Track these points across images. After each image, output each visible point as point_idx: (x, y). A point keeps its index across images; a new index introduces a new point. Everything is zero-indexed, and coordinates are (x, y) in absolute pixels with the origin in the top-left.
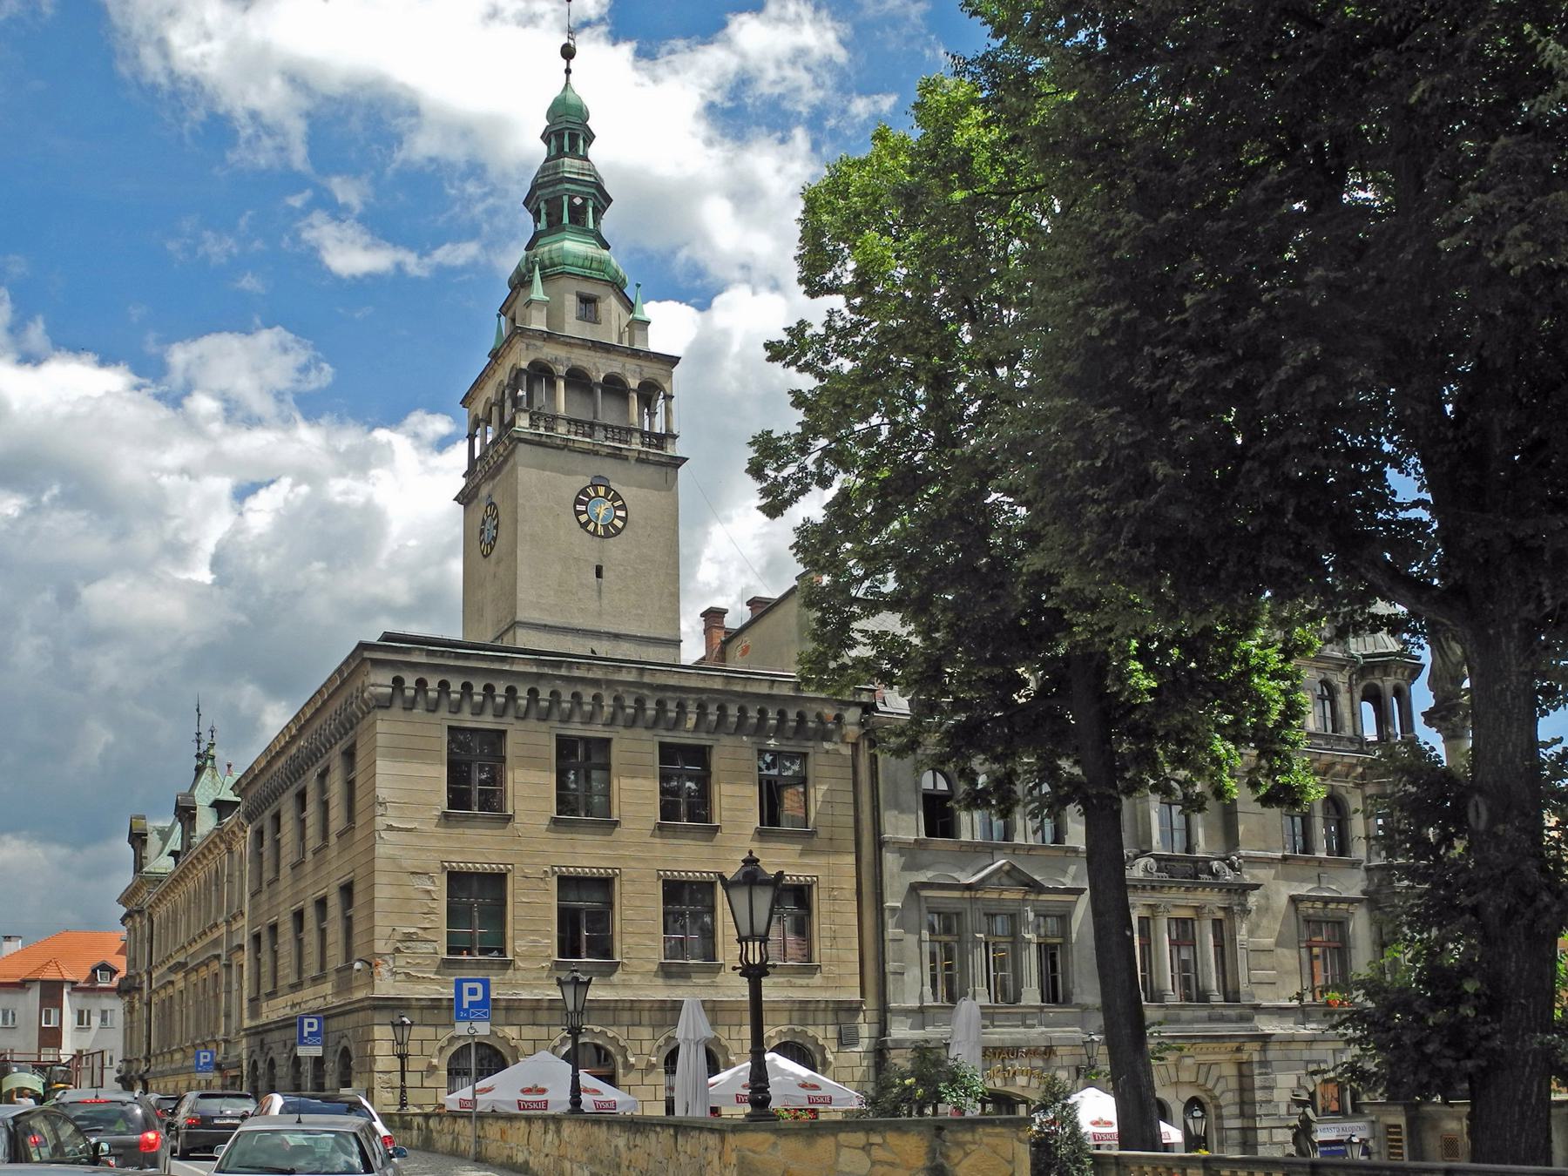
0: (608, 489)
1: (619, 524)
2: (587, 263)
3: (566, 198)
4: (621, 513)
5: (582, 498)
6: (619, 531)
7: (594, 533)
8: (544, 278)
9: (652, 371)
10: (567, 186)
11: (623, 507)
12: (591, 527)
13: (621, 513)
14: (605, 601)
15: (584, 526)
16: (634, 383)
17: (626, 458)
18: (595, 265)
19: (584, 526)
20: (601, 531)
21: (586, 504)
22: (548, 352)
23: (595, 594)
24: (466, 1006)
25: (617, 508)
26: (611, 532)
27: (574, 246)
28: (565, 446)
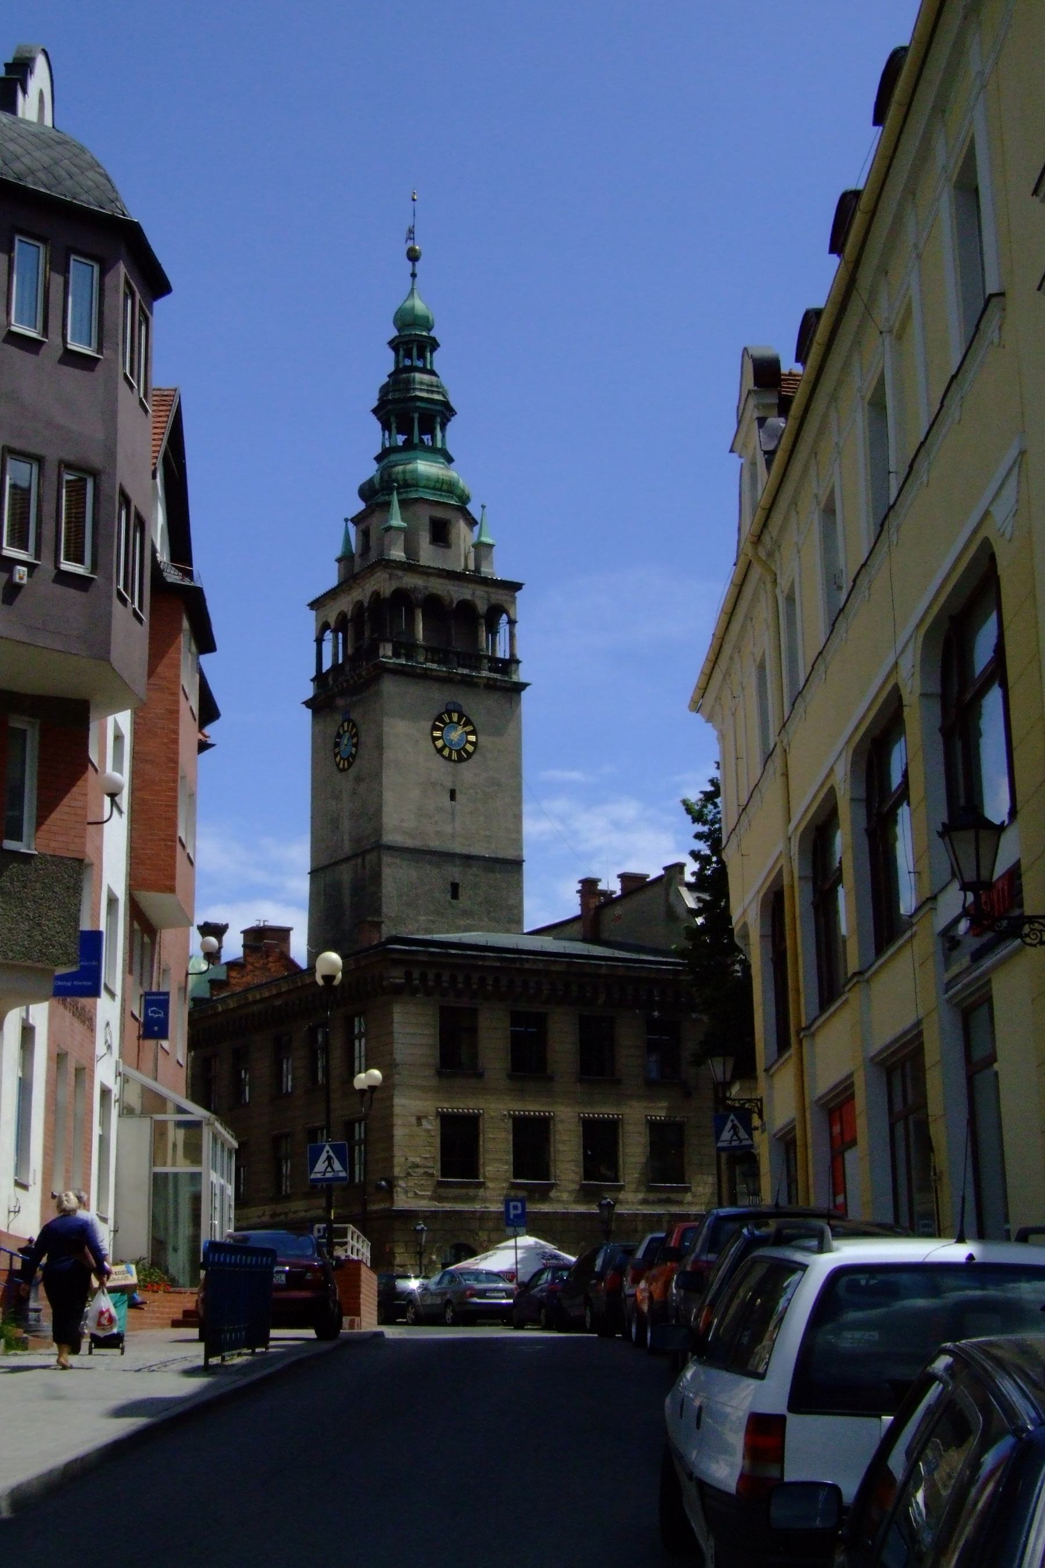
2: (438, 485)
6: (470, 755)
7: (449, 759)
8: (403, 504)
9: (499, 596)
10: (419, 404)
12: (446, 752)
15: (440, 751)
16: (482, 607)
18: (445, 487)
19: (440, 751)
20: (454, 756)
22: (411, 581)
24: (512, 1217)
26: (463, 756)
27: (425, 467)
28: (425, 676)
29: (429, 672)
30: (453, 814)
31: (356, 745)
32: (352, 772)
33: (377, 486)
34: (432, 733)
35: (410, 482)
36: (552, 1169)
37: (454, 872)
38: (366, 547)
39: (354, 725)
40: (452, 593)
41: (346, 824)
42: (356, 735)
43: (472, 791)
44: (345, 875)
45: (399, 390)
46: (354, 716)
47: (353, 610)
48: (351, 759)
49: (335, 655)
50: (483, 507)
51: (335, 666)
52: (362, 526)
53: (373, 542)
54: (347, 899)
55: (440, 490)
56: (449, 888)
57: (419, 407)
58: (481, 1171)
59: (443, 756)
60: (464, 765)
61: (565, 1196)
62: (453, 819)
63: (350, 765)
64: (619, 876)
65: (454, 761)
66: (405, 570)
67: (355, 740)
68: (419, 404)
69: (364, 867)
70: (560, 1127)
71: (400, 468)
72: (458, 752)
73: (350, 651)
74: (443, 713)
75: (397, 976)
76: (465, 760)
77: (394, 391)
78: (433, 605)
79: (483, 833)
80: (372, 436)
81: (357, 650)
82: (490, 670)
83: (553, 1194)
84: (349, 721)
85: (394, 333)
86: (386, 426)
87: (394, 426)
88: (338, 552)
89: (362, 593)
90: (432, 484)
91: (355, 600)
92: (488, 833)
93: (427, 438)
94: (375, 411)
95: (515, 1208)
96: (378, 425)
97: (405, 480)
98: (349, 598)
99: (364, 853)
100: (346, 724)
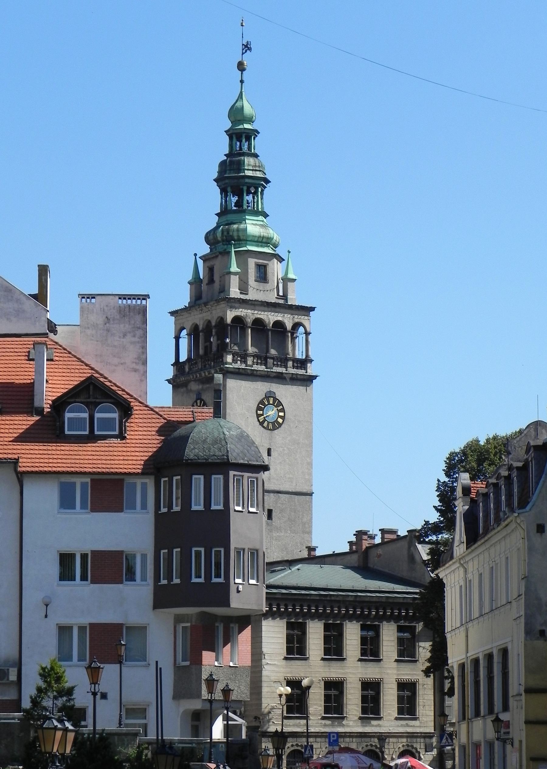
0: (275, 399)
1: (280, 420)
2: (260, 240)
3: (245, 188)
4: (281, 414)
5: (261, 406)
6: (280, 425)
7: (267, 428)
10: (247, 180)
11: (283, 410)
12: (265, 424)
13: (281, 414)
16: (289, 326)
17: (285, 378)
19: (261, 424)
20: (271, 426)
21: (262, 409)
25: (279, 411)
26: (276, 426)
29: (255, 372)
33: (219, 239)
34: (257, 412)
35: (242, 238)
38: (211, 281)
43: (281, 449)
45: (233, 170)
49: (189, 351)
51: (189, 359)
52: (209, 264)
53: (216, 278)
55: (261, 242)
57: (247, 183)
59: (264, 427)
65: (270, 430)
68: (247, 180)
71: (235, 226)
73: (201, 352)
74: (264, 399)
76: (278, 428)
77: (230, 170)
79: (288, 476)
82: (294, 367)
84: (201, 400)
86: (224, 191)
88: (190, 276)
90: (256, 239)
92: (291, 476)
97: (238, 236)
100: (199, 401)
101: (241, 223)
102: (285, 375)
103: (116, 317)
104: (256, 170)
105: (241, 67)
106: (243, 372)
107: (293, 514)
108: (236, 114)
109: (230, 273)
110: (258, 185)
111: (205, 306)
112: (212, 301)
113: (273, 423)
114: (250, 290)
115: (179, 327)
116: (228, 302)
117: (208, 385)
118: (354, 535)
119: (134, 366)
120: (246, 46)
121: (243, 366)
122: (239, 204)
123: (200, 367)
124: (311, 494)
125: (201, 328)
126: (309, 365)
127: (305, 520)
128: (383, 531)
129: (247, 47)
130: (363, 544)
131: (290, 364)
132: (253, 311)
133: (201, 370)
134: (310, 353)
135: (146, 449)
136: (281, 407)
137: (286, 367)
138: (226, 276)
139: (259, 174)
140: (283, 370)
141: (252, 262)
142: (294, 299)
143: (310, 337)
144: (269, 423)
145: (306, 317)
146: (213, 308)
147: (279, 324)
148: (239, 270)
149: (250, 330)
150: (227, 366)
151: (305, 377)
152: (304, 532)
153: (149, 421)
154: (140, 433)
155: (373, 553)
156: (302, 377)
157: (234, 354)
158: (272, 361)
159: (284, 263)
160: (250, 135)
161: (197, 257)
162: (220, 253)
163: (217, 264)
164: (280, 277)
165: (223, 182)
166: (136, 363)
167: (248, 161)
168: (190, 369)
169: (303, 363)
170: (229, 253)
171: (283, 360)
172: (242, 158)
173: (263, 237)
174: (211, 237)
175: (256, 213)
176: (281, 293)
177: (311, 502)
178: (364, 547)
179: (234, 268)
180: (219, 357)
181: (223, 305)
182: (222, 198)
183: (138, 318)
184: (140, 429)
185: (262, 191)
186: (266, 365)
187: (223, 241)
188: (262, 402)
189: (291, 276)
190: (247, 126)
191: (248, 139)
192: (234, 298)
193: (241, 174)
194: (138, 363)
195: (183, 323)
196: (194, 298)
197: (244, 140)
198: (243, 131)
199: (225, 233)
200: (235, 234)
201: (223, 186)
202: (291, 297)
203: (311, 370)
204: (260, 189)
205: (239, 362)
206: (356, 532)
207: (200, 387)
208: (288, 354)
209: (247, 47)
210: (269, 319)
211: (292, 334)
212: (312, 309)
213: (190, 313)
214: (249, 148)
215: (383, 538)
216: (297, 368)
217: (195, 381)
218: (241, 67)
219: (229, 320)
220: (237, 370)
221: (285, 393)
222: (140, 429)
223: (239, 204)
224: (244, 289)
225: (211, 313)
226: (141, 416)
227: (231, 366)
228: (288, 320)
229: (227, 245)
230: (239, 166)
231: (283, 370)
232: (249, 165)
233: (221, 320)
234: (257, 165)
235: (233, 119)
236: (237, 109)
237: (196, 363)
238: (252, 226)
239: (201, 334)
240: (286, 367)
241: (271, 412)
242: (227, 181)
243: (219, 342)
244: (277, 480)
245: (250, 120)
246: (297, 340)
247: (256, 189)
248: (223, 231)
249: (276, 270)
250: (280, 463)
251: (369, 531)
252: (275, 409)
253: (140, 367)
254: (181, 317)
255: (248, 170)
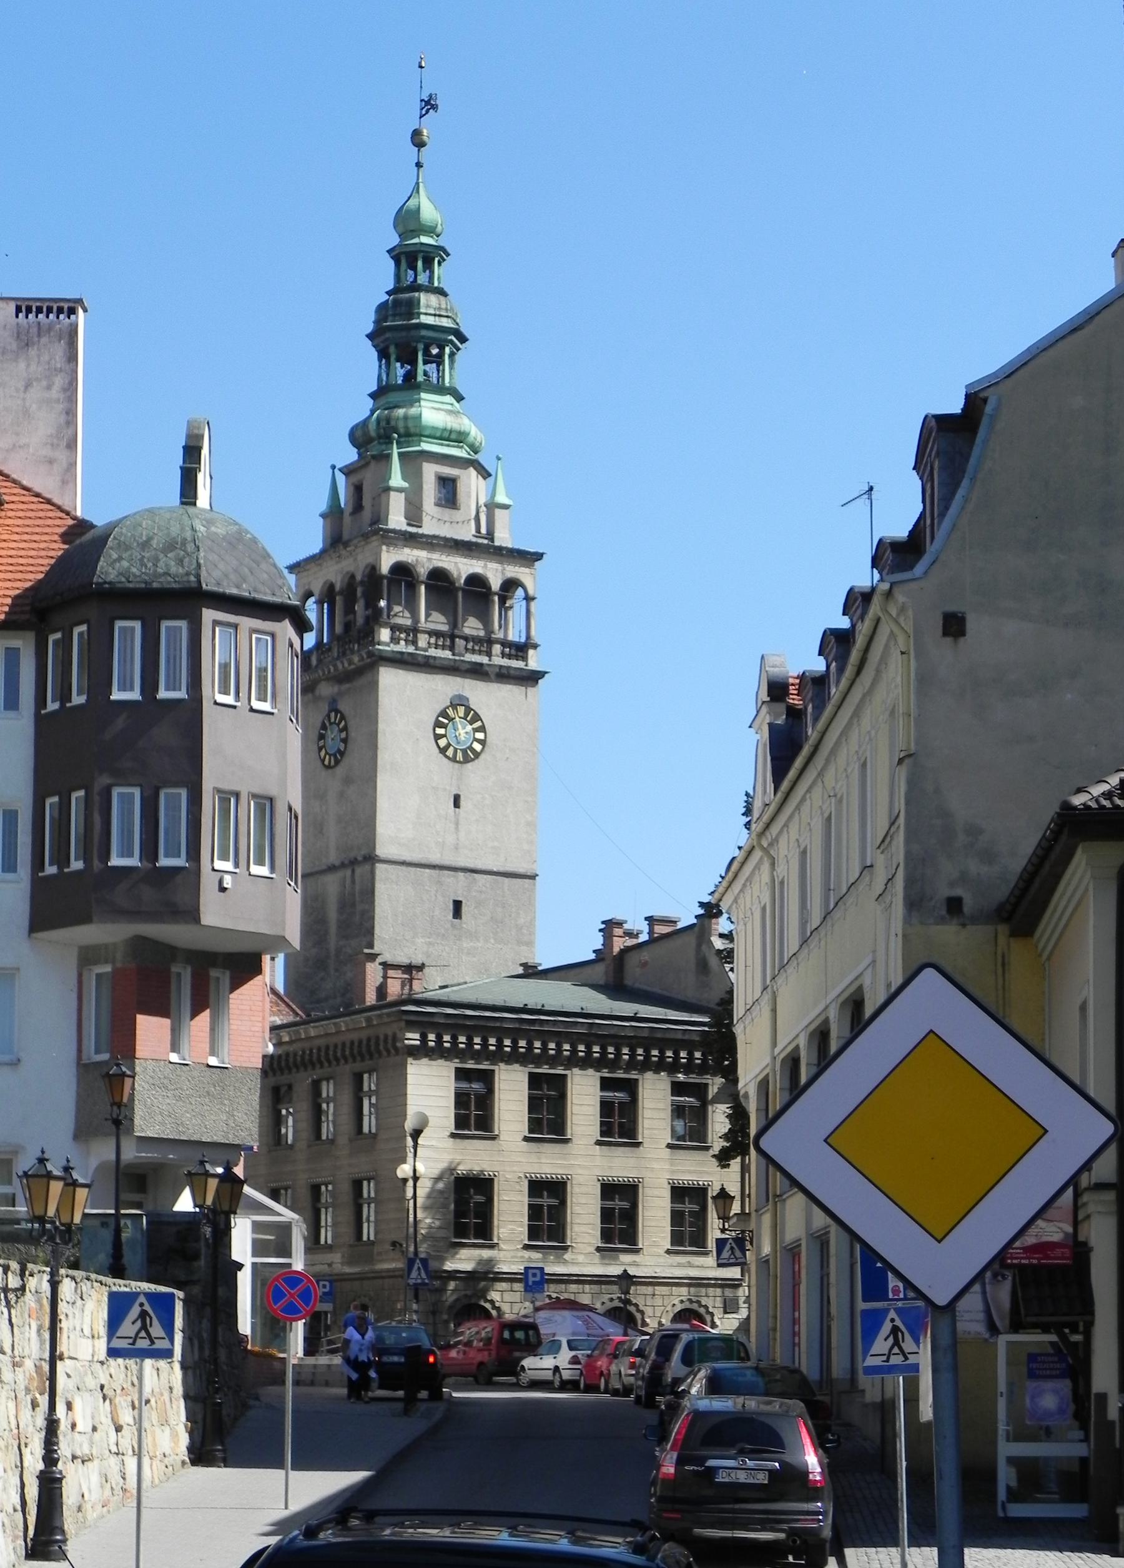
0: (468, 709)
1: (477, 747)
2: (446, 435)
3: (421, 346)
6: (477, 755)
7: (454, 759)
10: (424, 333)
11: (482, 729)
12: (450, 752)
14: (462, 834)
16: (495, 584)
23: (453, 826)
25: (476, 730)
26: (469, 756)
30: (457, 824)
31: (345, 741)
32: (340, 770)
33: (373, 434)
35: (412, 430)
36: (569, 1232)
37: (457, 886)
38: (358, 507)
39: (343, 718)
40: (460, 565)
41: (332, 831)
42: (345, 729)
44: (332, 885)
45: (400, 315)
46: (343, 706)
47: (342, 581)
48: (339, 756)
50: (499, 459)
53: (367, 502)
54: (333, 915)
56: (451, 907)
57: (423, 337)
58: (495, 1233)
60: (469, 765)
61: (581, 1258)
62: (457, 828)
63: (337, 762)
64: (646, 919)
65: (459, 762)
66: (406, 539)
67: (343, 735)
68: (424, 333)
69: (353, 882)
70: (576, 1189)
71: (401, 412)
72: (464, 751)
73: (339, 629)
75: (413, 1038)
76: (473, 760)
77: (394, 315)
78: (439, 579)
80: (365, 368)
81: (347, 626)
82: (503, 655)
83: (568, 1256)
84: (337, 711)
85: (394, 240)
87: (393, 358)
89: (354, 563)
90: (438, 434)
91: (347, 569)
92: (496, 844)
93: (432, 368)
94: (370, 336)
95: (534, 1275)
96: (374, 354)
98: (336, 567)
99: (353, 863)
100: (333, 715)
101: (412, 406)
102: (487, 668)
103: (9, 348)
104: (440, 316)
105: (417, 140)
106: (410, 659)
107: (499, 910)
108: (407, 221)
109: (388, 489)
110: (446, 340)
111: (345, 548)
112: (356, 537)
113: (464, 751)
114: (426, 519)
115: (302, 592)
116: (382, 536)
117: (347, 686)
118: (600, 930)
119: (46, 452)
120: (427, 103)
121: (411, 649)
122: (410, 377)
123: (336, 655)
124: (533, 877)
125: (338, 588)
126: (531, 652)
127: (521, 921)
128: (651, 920)
129: (429, 105)
130: (615, 944)
131: (497, 648)
132: (430, 555)
133: (338, 658)
134: (533, 633)
135: (19, 576)
136: (479, 724)
137: (489, 654)
138: (383, 495)
139: (445, 323)
140: (484, 660)
141: (430, 471)
142: (503, 538)
143: (533, 605)
144: (456, 750)
145: (527, 570)
146: (359, 550)
147: (476, 581)
148: (406, 485)
149: (423, 588)
150: (380, 647)
151: (524, 674)
152: (519, 942)
153: (40, 522)
154: (14, 545)
155: (632, 960)
156: (517, 673)
157: (394, 628)
158: (463, 642)
159: (491, 480)
160: (430, 256)
161: (336, 471)
162: (373, 457)
163: (368, 477)
164: (482, 501)
165: (382, 338)
166: (52, 445)
167: (427, 302)
168: (320, 661)
169: (520, 650)
170: (388, 457)
171: (485, 643)
172: (416, 294)
173: (451, 432)
174: (359, 433)
175: (440, 389)
176: (484, 531)
177: (533, 890)
178: (616, 950)
179: (396, 479)
180: (368, 634)
181: (374, 541)
182: (380, 366)
183: (59, 350)
184: (16, 537)
185: (452, 355)
186: (452, 648)
187: (379, 439)
188: (444, 714)
189: (501, 498)
190: (424, 239)
191: (428, 264)
192: (394, 531)
193: (414, 321)
194: (58, 445)
195: (309, 583)
196: (329, 541)
197: (420, 264)
198: (418, 248)
199: (383, 424)
200: (401, 424)
201: (382, 345)
202: (502, 535)
203: (534, 661)
204: (447, 350)
205: (402, 643)
206: (603, 922)
207: (336, 689)
208: (493, 632)
209: (429, 105)
210: (458, 570)
211: (503, 600)
212: (538, 556)
213: (320, 565)
214: (431, 278)
215: (651, 932)
216: (510, 657)
217: (328, 679)
218: (417, 140)
219: (385, 568)
220: (399, 656)
221: (484, 696)
222: (16, 537)
223: (410, 377)
224: (414, 514)
225: (355, 560)
226: (21, 514)
227: (387, 648)
228: (494, 573)
229: (386, 443)
230: (410, 308)
231: (484, 660)
232: (428, 306)
233: (373, 569)
234: (443, 306)
235: (401, 230)
236: (408, 211)
237: (329, 650)
238: (432, 411)
239: (337, 598)
240: (489, 654)
241: (464, 731)
242: (388, 335)
243: (369, 612)
244: (471, 850)
245: (431, 231)
246: (510, 613)
247: (442, 348)
248: (378, 420)
249: (472, 487)
250: (477, 820)
251: (626, 922)
252: (469, 728)
253: (61, 455)
254: (305, 574)
255: (426, 314)
